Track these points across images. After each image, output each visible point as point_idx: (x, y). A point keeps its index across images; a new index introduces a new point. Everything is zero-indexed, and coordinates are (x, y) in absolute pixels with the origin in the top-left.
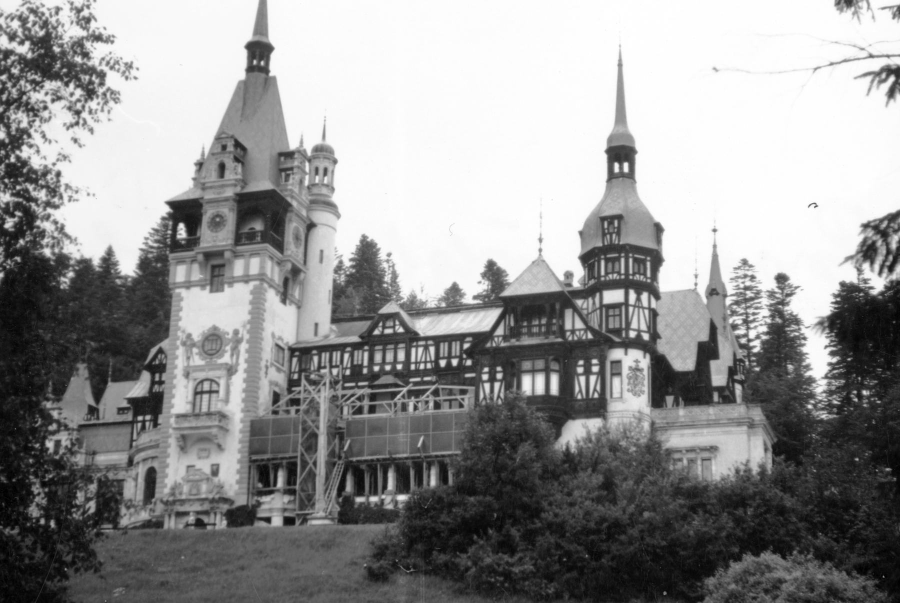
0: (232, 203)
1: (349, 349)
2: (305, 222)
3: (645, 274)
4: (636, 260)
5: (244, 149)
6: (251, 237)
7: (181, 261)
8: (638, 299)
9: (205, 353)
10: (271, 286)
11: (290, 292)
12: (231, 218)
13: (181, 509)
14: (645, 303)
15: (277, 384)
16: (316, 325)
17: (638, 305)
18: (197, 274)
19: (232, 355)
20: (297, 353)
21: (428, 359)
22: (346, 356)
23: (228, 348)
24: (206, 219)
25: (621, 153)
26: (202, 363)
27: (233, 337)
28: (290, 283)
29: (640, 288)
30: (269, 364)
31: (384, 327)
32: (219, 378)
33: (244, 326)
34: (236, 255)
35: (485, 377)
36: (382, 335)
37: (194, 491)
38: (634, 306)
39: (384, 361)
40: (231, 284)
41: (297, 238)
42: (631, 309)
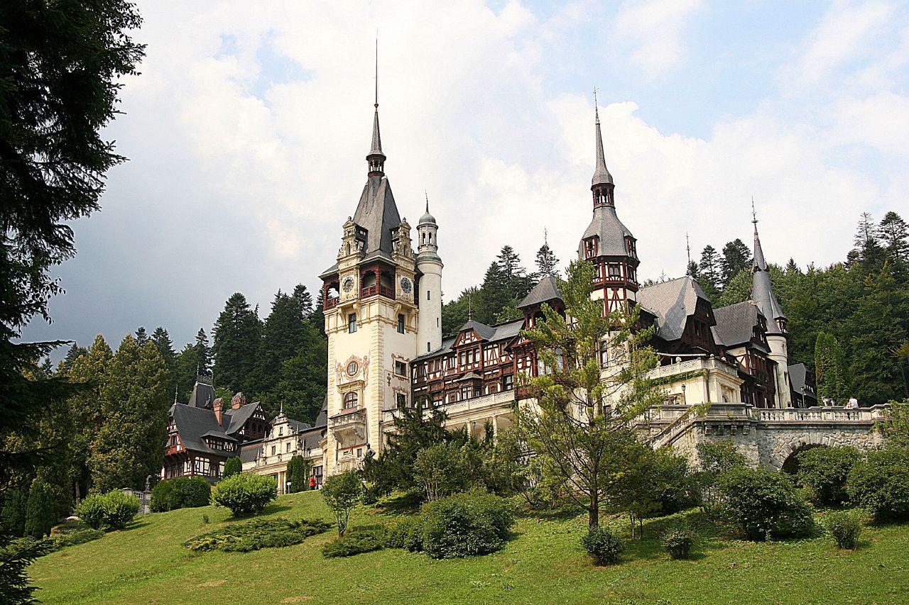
0: (354, 272)
1: (446, 358)
3: (619, 276)
4: (610, 266)
5: (366, 231)
6: (373, 292)
7: (330, 315)
8: (616, 295)
11: (406, 323)
12: (356, 279)
14: (621, 297)
17: (616, 298)
18: (341, 323)
20: (415, 366)
23: (362, 369)
24: (341, 284)
25: (604, 191)
26: (348, 381)
28: (406, 318)
29: (615, 286)
30: (391, 376)
33: (370, 353)
34: (361, 305)
35: (520, 366)
38: (612, 300)
39: (467, 363)
41: (405, 286)
42: (610, 302)
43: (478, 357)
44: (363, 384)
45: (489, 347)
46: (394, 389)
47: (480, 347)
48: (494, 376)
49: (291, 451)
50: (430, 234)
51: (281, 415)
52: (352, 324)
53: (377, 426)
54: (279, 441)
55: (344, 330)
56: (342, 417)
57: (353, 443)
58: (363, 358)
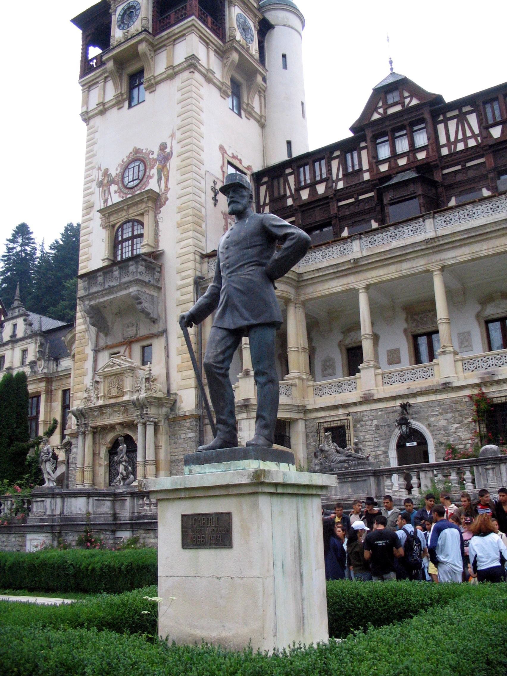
2: (256, 16)
9: (126, 187)
10: (209, 80)
11: (245, 99)
13: (100, 422)
16: (289, 143)
19: (159, 179)
20: (265, 179)
21: (469, 134)
22: (335, 164)
23: (154, 172)
27: (159, 155)
31: (387, 106)
33: (173, 135)
34: (156, 48)
36: (385, 118)
37: (114, 392)
40: (151, 88)
43: (421, 139)
44: (156, 200)
45: (449, 115)
47: (427, 116)
48: (471, 174)
49: (27, 363)
51: (16, 303)
52: (135, 91)
53: (191, 288)
54: (9, 346)
57: (131, 332)
58: (156, 150)
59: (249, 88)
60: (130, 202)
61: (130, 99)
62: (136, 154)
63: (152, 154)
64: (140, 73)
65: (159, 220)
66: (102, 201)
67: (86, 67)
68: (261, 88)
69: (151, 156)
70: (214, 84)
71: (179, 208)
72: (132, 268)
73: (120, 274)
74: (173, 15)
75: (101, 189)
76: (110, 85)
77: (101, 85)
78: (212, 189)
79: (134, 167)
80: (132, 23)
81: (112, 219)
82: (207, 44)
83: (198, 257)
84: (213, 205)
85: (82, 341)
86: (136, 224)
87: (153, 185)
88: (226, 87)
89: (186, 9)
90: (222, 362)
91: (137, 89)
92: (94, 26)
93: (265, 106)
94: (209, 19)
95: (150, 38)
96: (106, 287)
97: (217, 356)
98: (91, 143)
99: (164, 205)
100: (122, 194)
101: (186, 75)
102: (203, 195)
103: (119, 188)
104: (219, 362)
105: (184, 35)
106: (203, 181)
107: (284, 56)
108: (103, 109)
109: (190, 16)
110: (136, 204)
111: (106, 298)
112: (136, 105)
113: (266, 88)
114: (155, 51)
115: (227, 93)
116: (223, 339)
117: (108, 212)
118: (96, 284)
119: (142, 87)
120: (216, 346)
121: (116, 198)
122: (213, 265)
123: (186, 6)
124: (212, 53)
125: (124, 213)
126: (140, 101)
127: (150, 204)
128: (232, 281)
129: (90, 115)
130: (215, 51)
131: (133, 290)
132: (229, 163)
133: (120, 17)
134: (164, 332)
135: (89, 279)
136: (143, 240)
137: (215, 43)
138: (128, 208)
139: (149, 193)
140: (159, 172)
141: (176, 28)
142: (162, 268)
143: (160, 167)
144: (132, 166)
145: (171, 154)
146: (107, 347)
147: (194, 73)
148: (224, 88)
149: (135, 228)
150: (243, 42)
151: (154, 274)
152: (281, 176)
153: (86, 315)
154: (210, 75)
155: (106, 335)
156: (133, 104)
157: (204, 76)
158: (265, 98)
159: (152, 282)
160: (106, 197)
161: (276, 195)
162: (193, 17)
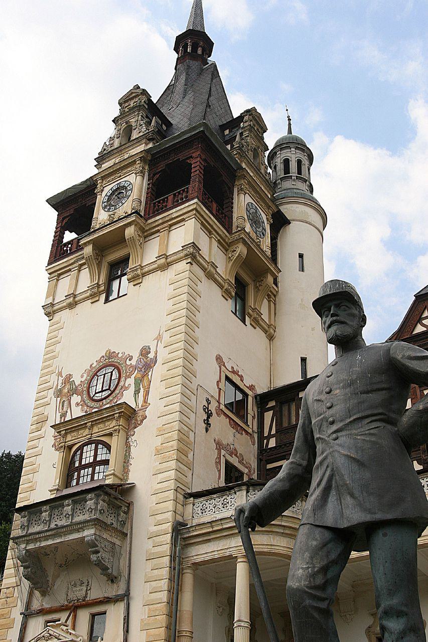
0: (138, 166)
2: (269, 207)
10: (210, 276)
15: (234, 453)
16: (304, 360)
19: (137, 392)
20: (272, 404)
23: (131, 381)
24: (101, 199)
27: (139, 361)
30: (213, 407)
32: (110, 435)
33: (159, 338)
34: (146, 234)
40: (136, 279)
44: (130, 417)
46: (219, 446)
50: (299, 162)
52: (116, 284)
53: (168, 538)
55: (92, 296)
56: (54, 503)
57: (78, 593)
58: (136, 355)
59: (257, 288)
60: (100, 414)
61: (108, 292)
62: (109, 359)
63: (130, 360)
64: (125, 260)
65: (131, 444)
66: (59, 415)
67: (59, 251)
68: (271, 291)
69: (128, 362)
70: (216, 281)
71: (159, 430)
72: (90, 503)
73: (73, 510)
74: (170, 198)
75: (59, 399)
76: (85, 273)
77: (74, 273)
78: (204, 410)
79: (104, 375)
80: (120, 204)
81: (69, 438)
82: (210, 232)
83: (181, 497)
84: (205, 430)
85: (8, 600)
86: (100, 446)
87: (128, 397)
88: (229, 285)
89: (187, 192)
90: (323, 587)
91: (118, 281)
92: (74, 207)
93: (275, 314)
94: (215, 206)
95: (141, 221)
96: (53, 526)
97: (313, 576)
98: (53, 340)
99: (140, 425)
100: (86, 407)
101: (183, 265)
102: (192, 416)
103: (83, 400)
104: (316, 588)
105: (183, 220)
106: (193, 398)
107: (301, 256)
108: (73, 302)
109: (193, 199)
110: (103, 421)
111: (50, 542)
112: (116, 299)
113: (277, 292)
114: (145, 238)
115: (230, 293)
116: (324, 545)
117: (64, 428)
118: (38, 521)
119: (124, 279)
120: (312, 558)
121: (77, 412)
122: (199, 509)
123: (188, 188)
124: (215, 244)
125: (87, 431)
126: (120, 295)
127: (122, 422)
128: (340, 445)
129: (55, 308)
130: (219, 242)
131: (88, 533)
132: (227, 378)
133: (107, 198)
134: (126, 597)
135: (30, 514)
136: (108, 468)
137: (220, 233)
138: (92, 426)
139: (121, 408)
140: (138, 383)
141: (174, 212)
142: (131, 508)
143: (140, 376)
144: (103, 371)
145: (155, 361)
146: (42, 612)
147: (192, 264)
148: (226, 286)
149: (99, 452)
150: (253, 235)
151: (119, 515)
152: (293, 400)
153: (20, 563)
154: (210, 268)
155: (44, 594)
156: (111, 298)
157: (204, 269)
158: (275, 304)
159: (115, 525)
160: (65, 410)
161: (285, 424)
162: (196, 200)
